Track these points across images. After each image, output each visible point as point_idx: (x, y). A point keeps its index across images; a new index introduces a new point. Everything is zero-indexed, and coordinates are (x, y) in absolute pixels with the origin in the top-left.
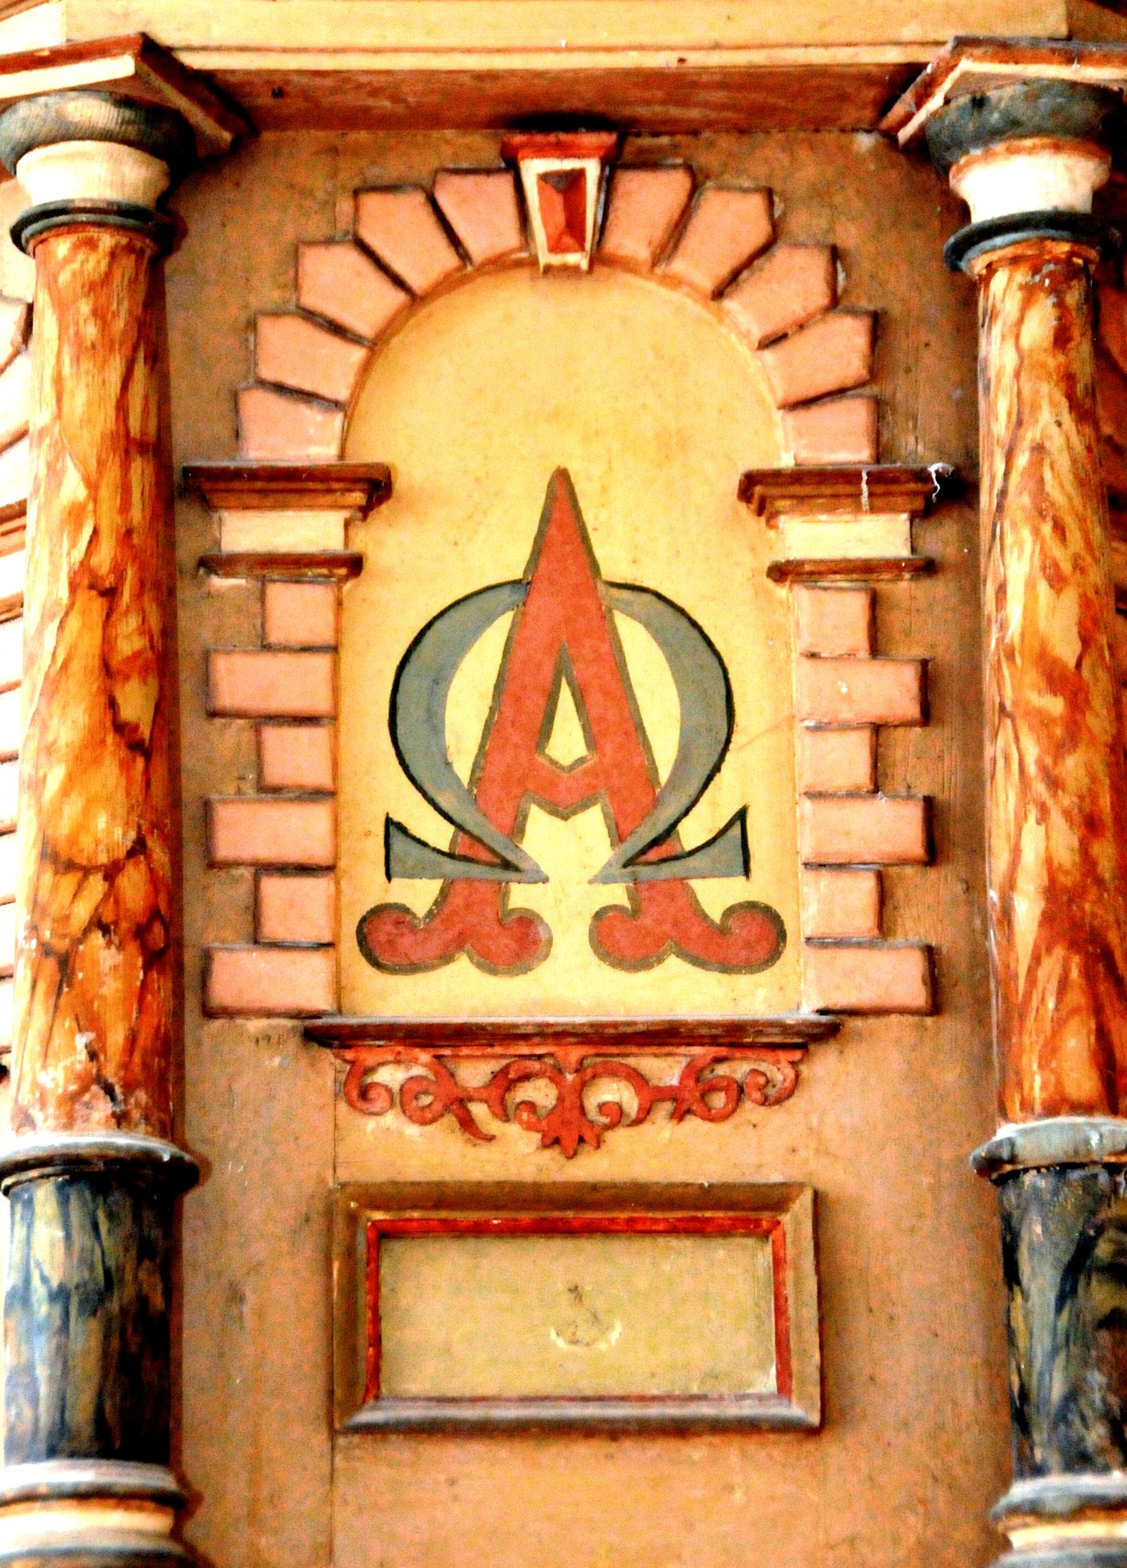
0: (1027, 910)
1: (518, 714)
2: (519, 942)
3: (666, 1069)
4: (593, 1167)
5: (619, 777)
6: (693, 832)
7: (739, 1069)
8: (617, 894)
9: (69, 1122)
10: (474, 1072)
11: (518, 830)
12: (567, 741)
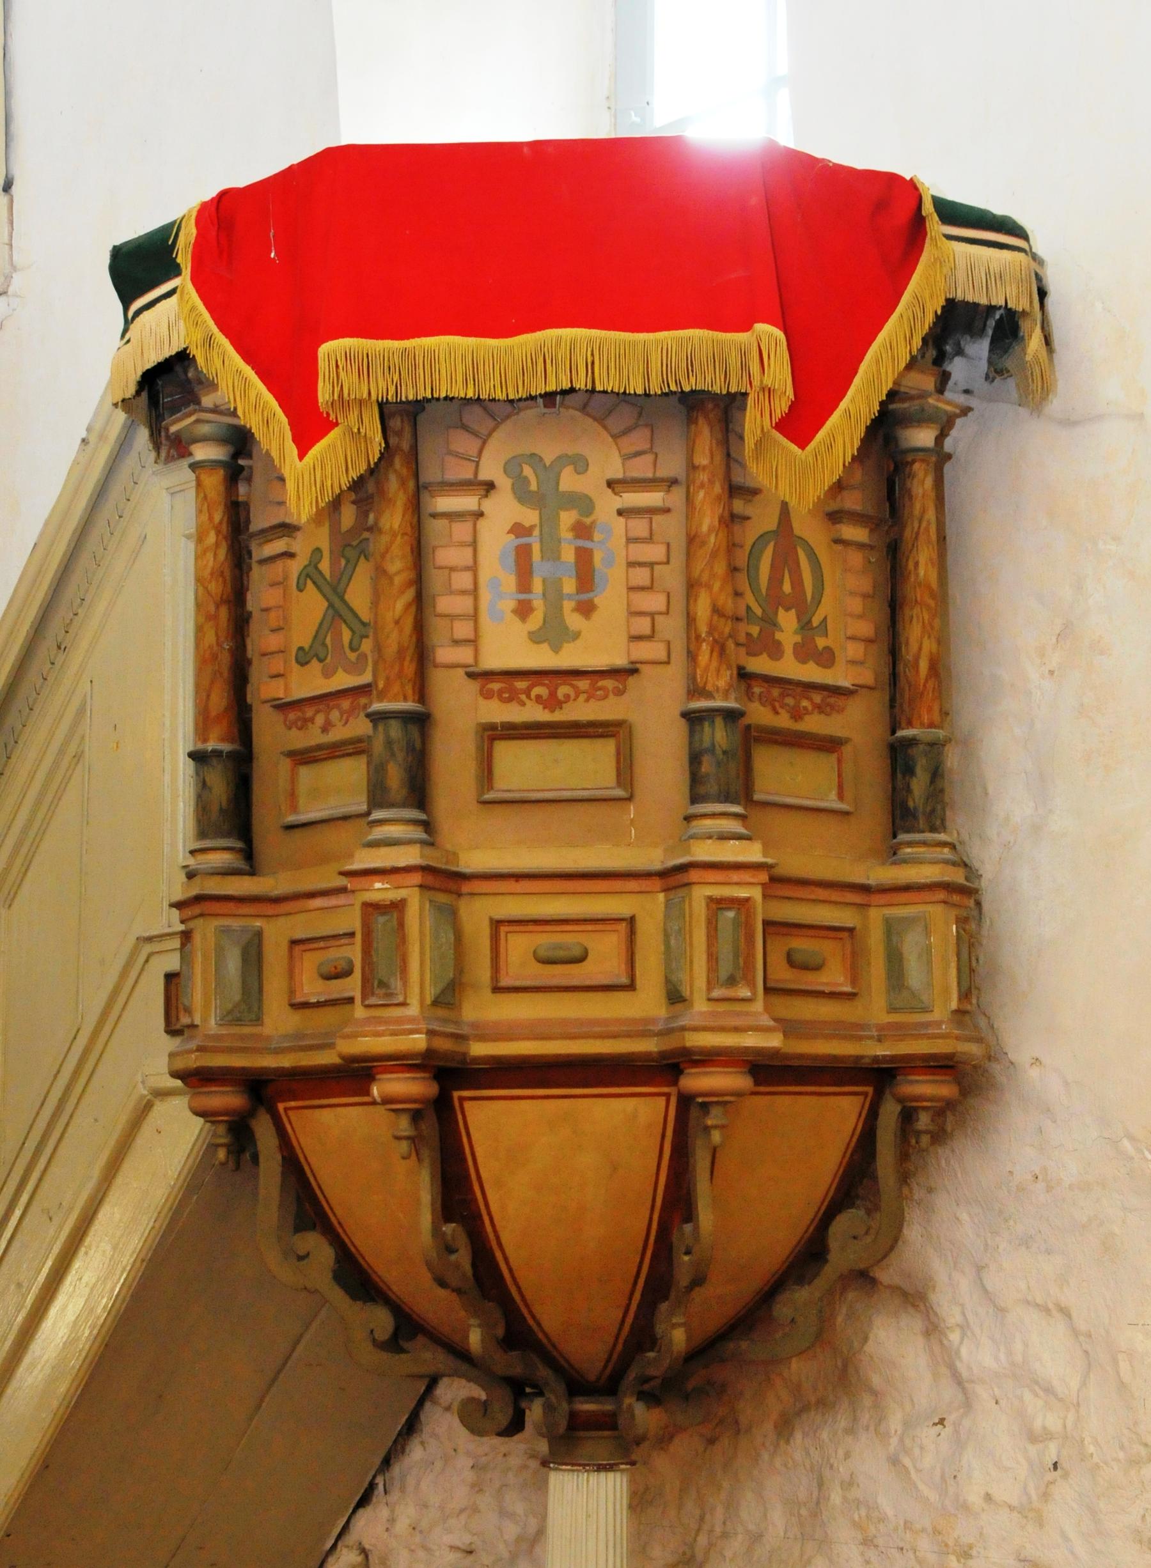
2: (775, 650)
3: (817, 698)
4: (801, 726)
6: (816, 622)
7: (832, 700)
8: (798, 639)
9: (726, 697)
10: (776, 692)
11: (776, 614)
12: (787, 587)
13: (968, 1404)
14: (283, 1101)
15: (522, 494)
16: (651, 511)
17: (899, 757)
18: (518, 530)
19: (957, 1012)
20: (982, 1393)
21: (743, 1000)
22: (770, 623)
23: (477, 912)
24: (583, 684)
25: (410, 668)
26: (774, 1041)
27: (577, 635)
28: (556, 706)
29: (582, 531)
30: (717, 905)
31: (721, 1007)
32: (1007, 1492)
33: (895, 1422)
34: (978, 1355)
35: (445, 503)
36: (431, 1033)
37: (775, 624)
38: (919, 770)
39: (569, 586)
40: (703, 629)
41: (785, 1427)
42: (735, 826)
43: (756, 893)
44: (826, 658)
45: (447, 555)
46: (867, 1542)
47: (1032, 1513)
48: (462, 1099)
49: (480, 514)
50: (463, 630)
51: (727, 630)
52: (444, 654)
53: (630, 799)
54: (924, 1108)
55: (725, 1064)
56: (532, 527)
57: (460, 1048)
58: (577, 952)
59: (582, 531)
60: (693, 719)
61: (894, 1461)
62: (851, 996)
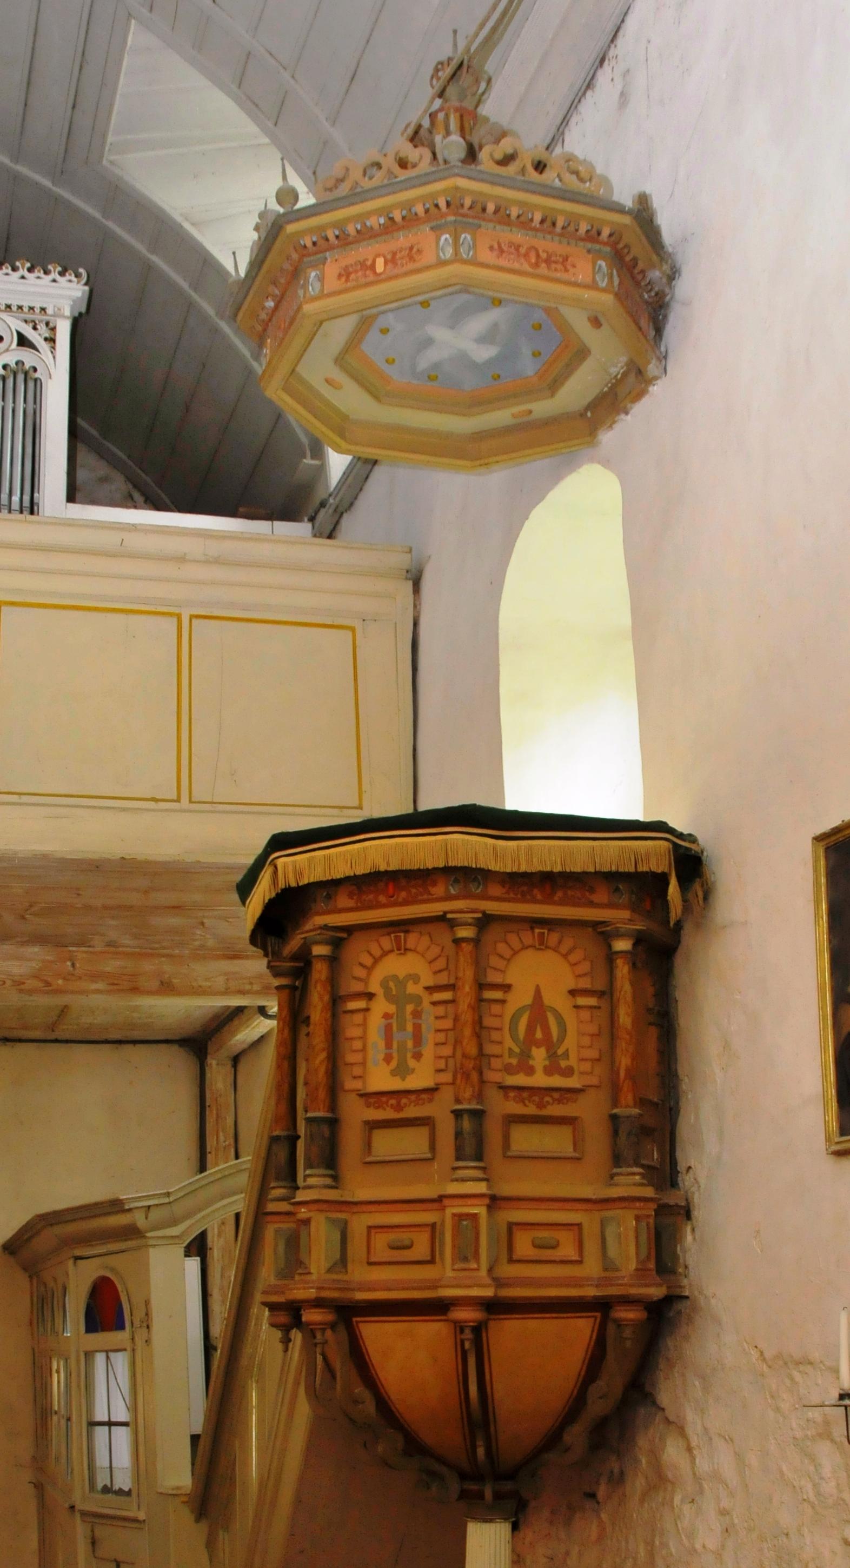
0: (622, 1074)
1: (530, 1029)
2: (530, 1071)
3: (556, 1095)
4: (544, 1112)
5: (548, 1042)
6: (560, 1052)
7: (568, 1095)
8: (547, 1063)
9: (469, 1103)
10: (525, 1094)
11: (530, 1050)
12: (539, 1035)
13: (701, 1491)
14: (356, 1316)
15: (389, 997)
18: (386, 1016)
19: (637, 1270)
22: (525, 1055)
23: (359, 1223)
24: (413, 1097)
25: (322, 1094)
26: (489, 1292)
27: (413, 1070)
28: (397, 1109)
29: (417, 1014)
30: (460, 1217)
32: (712, 1544)
33: (677, 1500)
34: (703, 1465)
35: (352, 1005)
36: (320, 1289)
37: (529, 1056)
38: (620, 1132)
39: (410, 1044)
40: (458, 1065)
42: (478, 1174)
43: (481, 1211)
44: (568, 1072)
45: (352, 1032)
47: (718, 1555)
48: (357, 1322)
49: (367, 1010)
50: (357, 1071)
51: (471, 1066)
52: (350, 1084)
53: (433, 1159)
54: (627, 1325)
55: (469, 1305)
56: (393, 1014)
57: (348, 1295)
58: (407, 1243)
59: (417, 1014)
60: (458, 1114)
62: (580, 1262)
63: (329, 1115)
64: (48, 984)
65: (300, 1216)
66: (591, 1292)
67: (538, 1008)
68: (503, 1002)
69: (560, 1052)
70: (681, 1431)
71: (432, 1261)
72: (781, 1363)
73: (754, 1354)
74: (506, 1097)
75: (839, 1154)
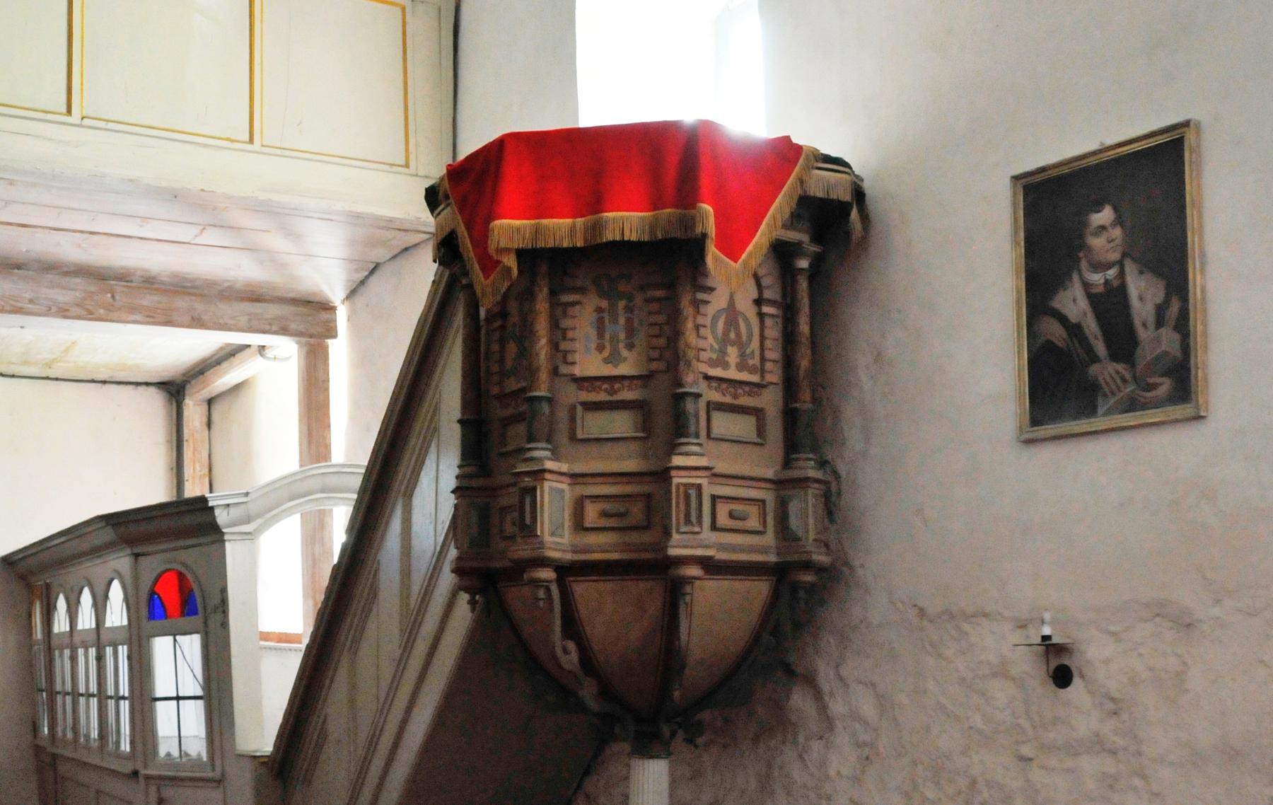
1: (726, 332)
2: (726, 366)
3: (747, 389)
4: (735, 402)
6: (748, 351)
10: (724, 386)
12: (732, 335)
15: (602, 294)
16: (659, 300)
17: (790, 417)
20: (839, 725)
21: (697, 533)
22: (723, 353)
24: (626, 383)
27: (625, 359)
31: (685, 536)
33: (801, 739)
34: (837, 707)
39: (622, 336)
41: (756, 739)
44: (752, 370)
46: (789, 793)
47: (857, 780)
52: (564, 369)
61: (800, 756)
63: (548, 395)
64: (90, 313)
65: (523, 485)
66: (772, 558)
67: (731, 311)
68: (707, 302)
69: (748, 351)
70: (810, 681)
71: (647, 528)
72: (945, 617)
73: (912, 614)
74: (710, 387)
75: (1029, 442)
